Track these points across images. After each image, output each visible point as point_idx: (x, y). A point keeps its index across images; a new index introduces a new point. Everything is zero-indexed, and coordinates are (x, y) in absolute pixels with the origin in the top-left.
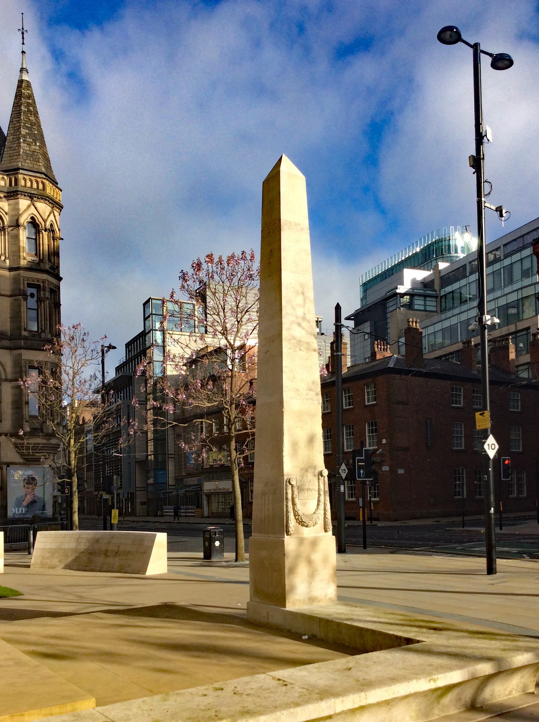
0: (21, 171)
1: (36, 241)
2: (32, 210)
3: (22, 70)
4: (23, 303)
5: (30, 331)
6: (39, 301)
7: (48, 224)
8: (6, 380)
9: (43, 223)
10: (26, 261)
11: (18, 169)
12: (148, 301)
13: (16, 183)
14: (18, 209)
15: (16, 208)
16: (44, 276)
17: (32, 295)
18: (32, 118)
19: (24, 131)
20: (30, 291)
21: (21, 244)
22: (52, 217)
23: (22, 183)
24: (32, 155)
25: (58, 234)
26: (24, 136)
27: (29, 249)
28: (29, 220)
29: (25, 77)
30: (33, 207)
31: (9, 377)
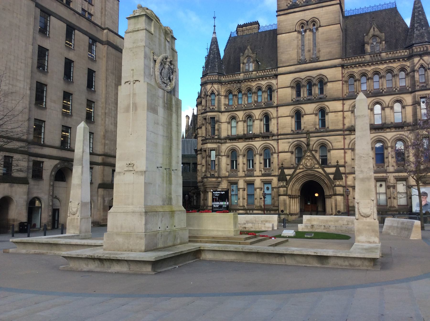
0: (415, 45)
2: (421, 61)
4: (418, 107)
9: (427, 66)
10: (418, 87)
11: (413, 44)
13: (412, 52)
14: (414, 63)
18: (421, 17)
21: (416, 79)
23: (415, 50)
26: (417, 27)
30: (421, 60)
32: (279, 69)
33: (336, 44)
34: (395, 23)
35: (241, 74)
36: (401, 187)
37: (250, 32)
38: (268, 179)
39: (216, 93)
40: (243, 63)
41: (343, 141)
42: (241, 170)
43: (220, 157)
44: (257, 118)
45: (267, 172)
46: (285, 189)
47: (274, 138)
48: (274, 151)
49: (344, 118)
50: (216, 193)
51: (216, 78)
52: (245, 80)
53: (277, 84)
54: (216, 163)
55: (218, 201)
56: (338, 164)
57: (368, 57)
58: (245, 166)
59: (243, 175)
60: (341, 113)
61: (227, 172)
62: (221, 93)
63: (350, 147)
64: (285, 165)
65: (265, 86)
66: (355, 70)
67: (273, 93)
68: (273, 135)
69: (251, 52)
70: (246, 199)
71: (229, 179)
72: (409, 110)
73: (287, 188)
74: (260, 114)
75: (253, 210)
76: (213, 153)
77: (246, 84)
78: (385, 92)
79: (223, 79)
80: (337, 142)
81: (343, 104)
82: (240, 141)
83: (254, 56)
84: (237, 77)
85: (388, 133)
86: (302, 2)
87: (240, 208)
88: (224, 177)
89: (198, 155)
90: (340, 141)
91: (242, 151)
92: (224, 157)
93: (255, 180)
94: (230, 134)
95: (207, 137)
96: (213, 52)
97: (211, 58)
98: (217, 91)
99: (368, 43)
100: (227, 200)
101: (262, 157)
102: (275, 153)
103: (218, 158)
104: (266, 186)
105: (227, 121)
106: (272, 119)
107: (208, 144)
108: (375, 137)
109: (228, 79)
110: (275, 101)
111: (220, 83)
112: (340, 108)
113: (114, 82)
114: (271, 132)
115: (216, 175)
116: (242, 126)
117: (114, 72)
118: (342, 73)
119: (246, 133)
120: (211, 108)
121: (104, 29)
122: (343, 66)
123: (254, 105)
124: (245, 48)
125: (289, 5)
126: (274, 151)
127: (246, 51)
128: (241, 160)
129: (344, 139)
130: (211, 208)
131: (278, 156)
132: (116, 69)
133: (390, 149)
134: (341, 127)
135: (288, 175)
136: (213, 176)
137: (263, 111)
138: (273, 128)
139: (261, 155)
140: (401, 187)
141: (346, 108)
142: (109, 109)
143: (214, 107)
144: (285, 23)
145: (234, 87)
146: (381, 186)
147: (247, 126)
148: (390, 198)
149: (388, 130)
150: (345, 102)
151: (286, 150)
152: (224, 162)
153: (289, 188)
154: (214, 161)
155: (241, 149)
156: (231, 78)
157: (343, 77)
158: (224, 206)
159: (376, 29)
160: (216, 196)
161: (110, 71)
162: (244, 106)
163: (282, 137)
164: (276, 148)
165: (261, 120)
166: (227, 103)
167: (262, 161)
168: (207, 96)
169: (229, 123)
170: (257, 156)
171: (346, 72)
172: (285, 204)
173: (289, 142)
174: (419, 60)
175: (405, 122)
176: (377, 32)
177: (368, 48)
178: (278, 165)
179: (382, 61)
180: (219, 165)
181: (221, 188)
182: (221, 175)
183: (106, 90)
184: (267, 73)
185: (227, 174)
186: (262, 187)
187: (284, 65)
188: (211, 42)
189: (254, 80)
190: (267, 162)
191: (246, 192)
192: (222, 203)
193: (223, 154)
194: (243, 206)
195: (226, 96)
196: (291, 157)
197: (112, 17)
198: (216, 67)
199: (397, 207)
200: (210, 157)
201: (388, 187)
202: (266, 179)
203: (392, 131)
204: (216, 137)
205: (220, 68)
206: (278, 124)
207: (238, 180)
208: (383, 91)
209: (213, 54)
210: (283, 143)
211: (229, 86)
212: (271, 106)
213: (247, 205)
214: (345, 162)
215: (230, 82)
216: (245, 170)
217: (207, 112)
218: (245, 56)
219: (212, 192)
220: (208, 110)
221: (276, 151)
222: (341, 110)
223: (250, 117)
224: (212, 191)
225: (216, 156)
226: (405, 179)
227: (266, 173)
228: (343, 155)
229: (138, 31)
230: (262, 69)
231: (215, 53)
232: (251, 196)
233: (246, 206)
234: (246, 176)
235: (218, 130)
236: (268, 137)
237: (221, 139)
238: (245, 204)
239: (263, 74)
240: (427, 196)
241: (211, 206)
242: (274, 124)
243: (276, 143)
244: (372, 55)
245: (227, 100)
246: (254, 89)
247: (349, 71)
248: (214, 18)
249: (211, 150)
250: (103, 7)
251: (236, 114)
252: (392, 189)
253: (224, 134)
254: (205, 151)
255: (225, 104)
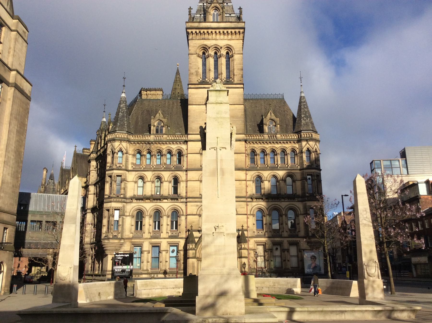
1: (309, 157)
2: (308, 145)
3: (301, 92)
4: (306, 182)
5: (309, 193)
6: (313, 180)
7: (314, 149)
8: (301, 214)
12: (372, 162)
13: (301, 137)
15: (301, 146)
16: (314, 171)
17: (309, 179)
18: (306, 110)
19: (303, 116)
20: (308, 177)
22: (316, 146)
23: (303, 136)
24: (307, 124)
25: (319, 152)
26: (303, 118)
27: (307, 160)
28: (306, 149)
29: (303, 95)
31: (302, 213)
32: (189, 136)
33: (241, 122)
34: (284, 112)
35: (151, 136)
36: (293, 251)
37: (154, 97)
38: (174, 242)
39: (125, 151)
40: (154, 126)
41: (246, 207)
42: (147, 232)
43: (125, 217)
44: (166, 180)
45: (174, 234)
46: (194, 251)
47: (182, 200)
48: (182, 214)
49: (247, 186)
50: (119, 255)
51: (125, 137)
52: (156, 142)
53: (187, 149)
54: (120, 223)
55: (121, 265)
56: (243, 229)
57: (266, 137)
58: (151, 227)
59: (149, 237)
60: (245, 182)
61: (131, 233)
62: (129, 151)
63: (252, 213)
64: (194, 228)
65: (175, 149)
66: (256, 145)
67: (182, 157)
68: (182, 198)
69: (162, 116)
70: (150, 262)
71: (133, 240)
72: (298, 184)
73: (196, 250)
74: (169, 176)
75: (157, 273)
76: (117, 213)
77: (155, 145)
78: (280, 167)
79: (131, 138)
80: (241, 208)
81: (246, 174)
82: (147, 201)
83: (165, 120)
84: (147, 138)
85: (283, 203)
86: (211, 81)
87: (143, 272)
88: (127, 239)
89: (88, 214)
90: (244, 208)
91: (149, 212)
92: (128, 217)
93: (161, 242)
94: (136, 194)
95: (111, 196)
96: (122, 110)
97: (119, 116)
98: (126, 150)
99: (266, 125)
100: (131, 264)
101: (169, 219)
102: (183, 215)
103: (123, 218)
104: (172, 248)
105: (134, 180)
106: (181, 182)
107: (112, 203)
108: (272, 205)
109: (137, 138)
110: (185, 165)
111: (129, 141)
112: (244, 178)
113: (16, 127)
114: (180, 195)
115: (119, 236)
116: (150, 187)
117: (18, 117)
118: (245, 147)
119: (153, 194)
120: (118, 165)
121: (11, 70)
122: (246, 141)
123: (163, 167)
124: (157, 112)
125: (199, 81)
126: (182, 214)
127: (158, 115)
128: (148, 222)
129: (247, 205)
130: (111, 273)
131: (186, 218)
132: (19, 114)
133: (284, 216)
134: (244, 194)
135: (197, 238)
136: (115, 237)
137: (172, 173)
138: (182, 190)
139: (168, 217)
140: (293, 251)
141: (249, 178)
142: (8, 157)
143: (121, 165)
144: (196, 96)
145: (144, 148)
146: (277, 249)
147: (155, 187)
148: (285, 261)
149: (283, 200)
150: (247, 172)
151: (194, 213)
152: (129, 223)
153: (197, 251)
154: (118, 221)
155: (148, 209)
156: (140, 138)
157: (246, 150)
158: (127, 270)
159: (272, 114)
160: (118, 260)
161: (14, 115)
162: (153, 167)
163: (191, 200)
164: (184, 211)
165: (170, 182)
166: (135, 162)
167: (169, 223)
168: (115, 153)
169: (136, 182)
170: (165, 218)
171: (248, 146)
172: (193, 267)
173: (197, 206)
174: (306, 144)
175: (296, 194)
176: (273, 117)
177: (266, 128)
178: (186, 227)
179: (278, 141)
180: (123, 225)
181: (123, 250)
182: (125, 237)
183: (8, 136)
184: (178, 138)
185: (131, 235)
186: (168, 249)
187: (194, 133)
188: (121, 101)
189: (164, 143)
190: (175, 224)
191: (150, 255)
192: (125, 267)
193: (128, 214)
194: (147, 270)
195: (134, 155)
196: (199, 221)
197: (19, 58)
198: (125, 125)
199: (290, 268)
200: (113, 216)
201: (283, 250)
202: (172, 242)
203: (286, 201)
204: (122, 196)
205: (128, 126)
206: (187, 187)
207: (143, 242)
208: (278, 166)
209: (122, 113)
210: (192, 206)
211: (138, 145)
212: (179, 169)
213: (151, 269)
214: (248, 227)
215: (138, 142)
216: (151, 231)
217: (113, 170)
218: (156, 119)
219: (115, 255)
220: (114, 167)
221: (184, 214)
222: (245, 179)
223: (159, 178)
224: (115, 253)
225: (120, 216)
226: (296, 244)
227: (172, 235)
228: (246, 220)
229: (221, 103)
230: (171, 133)
231: (124, 112)
232: (157, 259)
233: (150, 270)
234: (152, 238)
235: (124, 189)
236: (177, 199)
237: (126, 199)
238: (149, 268)
239: (173, 138)
240: (316, 259)
241: (109, 271)
242: (183, 187)
243: (184, 206)
244: (270, 135)
245: (135, 159)
246: (164, 152)
247: (251, 146)
248: (124, 78)
249: (115, 210)
250: (12, 47)
251: (144, 174)
252: (286, 252)
253: (129, 194)
254: (108, 210)
255: (132, 163)
